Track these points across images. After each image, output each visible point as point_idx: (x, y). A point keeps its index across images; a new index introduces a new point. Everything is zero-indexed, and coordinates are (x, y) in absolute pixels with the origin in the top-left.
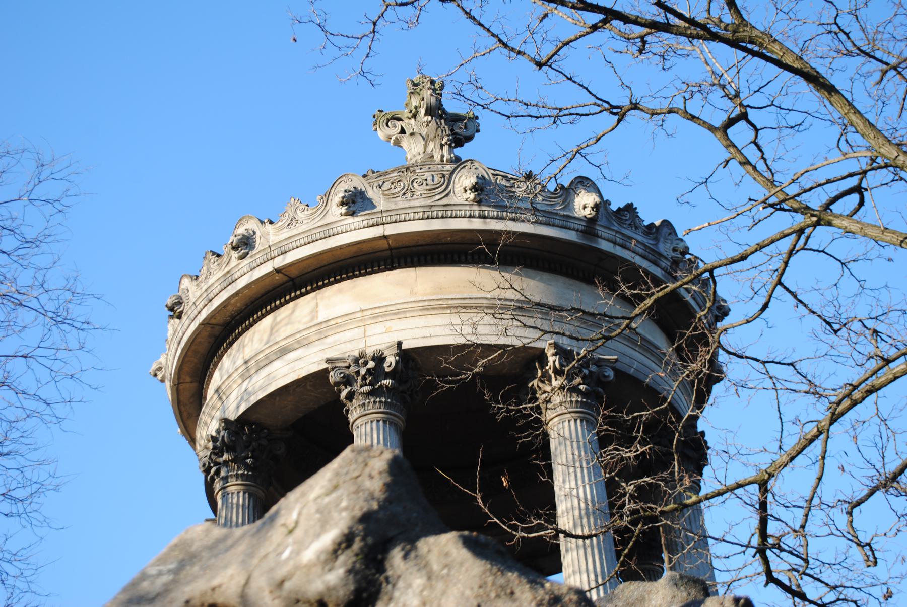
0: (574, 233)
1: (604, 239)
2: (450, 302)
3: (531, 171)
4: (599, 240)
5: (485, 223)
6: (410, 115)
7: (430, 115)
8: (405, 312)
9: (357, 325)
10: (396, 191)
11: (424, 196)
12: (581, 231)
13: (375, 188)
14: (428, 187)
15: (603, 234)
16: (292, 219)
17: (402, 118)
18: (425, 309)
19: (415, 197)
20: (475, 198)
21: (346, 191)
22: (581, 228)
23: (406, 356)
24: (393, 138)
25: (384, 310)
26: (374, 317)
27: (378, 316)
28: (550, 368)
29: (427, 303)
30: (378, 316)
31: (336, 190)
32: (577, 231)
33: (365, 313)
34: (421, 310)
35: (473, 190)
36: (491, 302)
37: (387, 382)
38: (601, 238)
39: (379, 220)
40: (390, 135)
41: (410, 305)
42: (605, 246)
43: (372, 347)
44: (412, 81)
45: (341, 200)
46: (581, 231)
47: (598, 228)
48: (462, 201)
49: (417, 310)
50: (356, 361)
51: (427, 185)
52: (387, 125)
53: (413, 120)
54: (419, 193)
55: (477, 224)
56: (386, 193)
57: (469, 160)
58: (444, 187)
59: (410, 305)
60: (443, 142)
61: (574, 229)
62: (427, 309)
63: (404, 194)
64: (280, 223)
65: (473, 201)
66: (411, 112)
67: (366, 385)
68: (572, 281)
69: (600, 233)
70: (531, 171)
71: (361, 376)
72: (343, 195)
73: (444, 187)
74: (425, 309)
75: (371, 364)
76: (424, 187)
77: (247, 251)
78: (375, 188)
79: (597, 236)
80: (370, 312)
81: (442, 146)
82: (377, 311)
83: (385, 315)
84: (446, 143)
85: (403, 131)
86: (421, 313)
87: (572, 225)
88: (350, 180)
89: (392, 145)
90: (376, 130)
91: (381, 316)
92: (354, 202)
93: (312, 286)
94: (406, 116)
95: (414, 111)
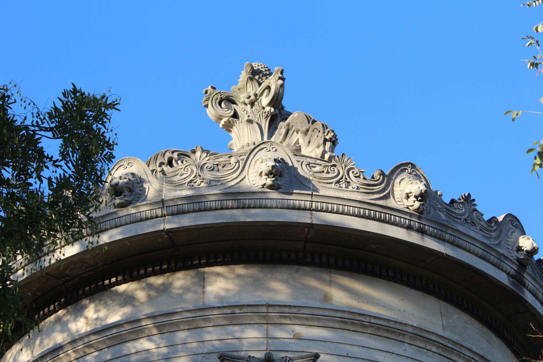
0: (505, 275)
1: (529, 291)
2: (373, 321)
3: (469, 194)
4: (526, 290)
5: (423, 239)
6: (247, 101)
7: (273, 107)
8: (319, 320)
9: (258, 321)
10: (331, 175)
11: (361, 190)
12: (512, 276)
13: (304, 166)
14: (365, 182)
15: (530, 284)
16: (196, 176)
17: (236, 101)
18: (343, 321)
19: (350, 188)
20: (419, 208)
21: (275, 160)
22: (512, 272)
24: (225, 119)
25: (295, 310)
26: (281, 316)
27: (286, 317)
29: (346, 315)
30: (286, 317)
31: (257, 157)
32: (508, 274)
33: (271, 310)
34: (338, 322)
35: (420, 198)
36: (416, 332)
38: (527, 288)
39: (308, 204)
40: (221, 116)
41: (327, 313)
42: (529, 297)
43: (280, 353)
44: (252, 67)
45: (270, 168)
46: (512, 276)
47: (525, 275)
49: (334, 321)
51: (364, 178)
52: (220, 104)
53: (249, 106)
54: (355, 186)
55: (414, 238)
56: (316, 175)
57: (407, 164)
58: (383, 185)
59: (327, 313)
60: (328, 137)
61: (505, 272)
62: (345, 323)
63: (338, 182)
64: (178, 176)
65: (417, 210)
66: (249, 97)
68: (485, 329)
69: (527, 283)
70: (469, 194)
72: (274, 164)
73: (383, 185)
74: (343, 321)
76: (361, 180)
77: (131, 199)
78: (304, 166)
79: (524, 285)
80: (277, 310)
81: (325, 140)
82: (287, 310)
83: (296, 318)
84: (331, 139)
85: (235, 116)
86: (337, 325)
87: (505, 267)
88: (274, 149)
89: (221, 126)
90: (207, 106)
91: (290, 318)
92: (281, 176)
93: (200, 260)
94: (242, 100)
95: (253, 97)
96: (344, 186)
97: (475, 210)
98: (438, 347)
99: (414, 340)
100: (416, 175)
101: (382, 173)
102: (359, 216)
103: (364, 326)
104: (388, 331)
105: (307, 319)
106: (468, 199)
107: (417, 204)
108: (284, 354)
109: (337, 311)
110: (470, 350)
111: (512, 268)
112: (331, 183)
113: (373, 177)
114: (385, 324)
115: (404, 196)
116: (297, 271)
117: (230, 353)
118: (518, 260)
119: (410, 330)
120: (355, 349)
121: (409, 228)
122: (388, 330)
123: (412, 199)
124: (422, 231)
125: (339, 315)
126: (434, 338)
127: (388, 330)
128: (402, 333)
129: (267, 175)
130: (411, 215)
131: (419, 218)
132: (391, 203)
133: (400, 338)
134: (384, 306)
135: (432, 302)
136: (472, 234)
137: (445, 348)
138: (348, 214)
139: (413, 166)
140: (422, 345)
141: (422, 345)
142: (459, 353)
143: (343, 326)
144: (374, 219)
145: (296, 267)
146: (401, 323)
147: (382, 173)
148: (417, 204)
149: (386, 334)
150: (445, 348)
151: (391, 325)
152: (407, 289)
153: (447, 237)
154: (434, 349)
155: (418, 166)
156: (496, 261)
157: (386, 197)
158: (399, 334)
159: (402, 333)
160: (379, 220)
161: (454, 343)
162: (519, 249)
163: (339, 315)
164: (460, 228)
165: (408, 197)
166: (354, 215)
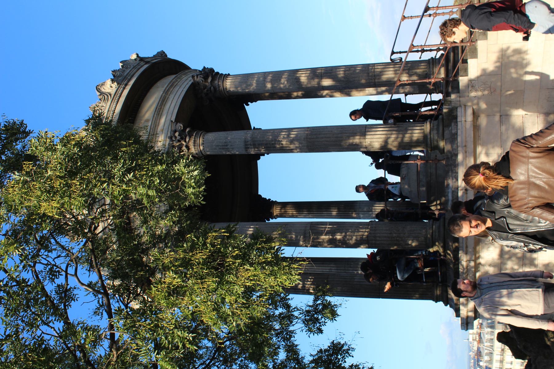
19: (105, 106)
22: (144, 63)
23: (177, 120)
25: (151, 130)
28: (202, 81)
29: (156, 113)
37: (188, 130)
41: (154, 120)
48: (115, 90)
57: (97, 88)
65: (118, 84)
71: (181, 140)
75: (177, 134)
83: (154, 130)
86: (159, 117)
96: (103, 108)
99: (168, 94)
100: (102, 85)
101: (100, 95)
102: (117, 103)
103: (161, 108)
104: (164, 101)
105: (155, 127)
106: (114, 71)
107: (116, 83)
109: (154, 116)
110: (173, 79)
111: (142, 63)
113: (100, 99)
115: (111, 88)
118: (140, 61)
119: (164, 94)
120: (177, 89)
121: (124, 88)
122: (163, 101)
123: (113, 85)
124: (126, 85)
125: (155, 116)
126: (168, 88)
127: (163, 101)
128: (165, 97)
130: (119, 87)
131: (121, 84)
132: (113, 93)
133: (167, 98)
134: (153, 103)
135: (152, 90)
136: (128, 71)
137: (172, 86)
138: (116, 107)
139: (98, 86)
140: (170, 92)
141: (170, 92)
142: (174, 83)
143: (160, 115)
144: (119, 99)
146: (161, 97)
147: (100, 95)
148: (116, 83)
149: (165, 102)
150: (172, 86)
152: (148, 94)
153: (129, 78)
154: (172, 89)
155: (98, 84)
156: (140, 66)
157: (110, 95)
159: (165, 97)
160: (120, 97)
161: (170, 83)
162: (135, 60)
163: (155, 116)
164: (126, 74)
165: (112, 87)
166: (116, 105)
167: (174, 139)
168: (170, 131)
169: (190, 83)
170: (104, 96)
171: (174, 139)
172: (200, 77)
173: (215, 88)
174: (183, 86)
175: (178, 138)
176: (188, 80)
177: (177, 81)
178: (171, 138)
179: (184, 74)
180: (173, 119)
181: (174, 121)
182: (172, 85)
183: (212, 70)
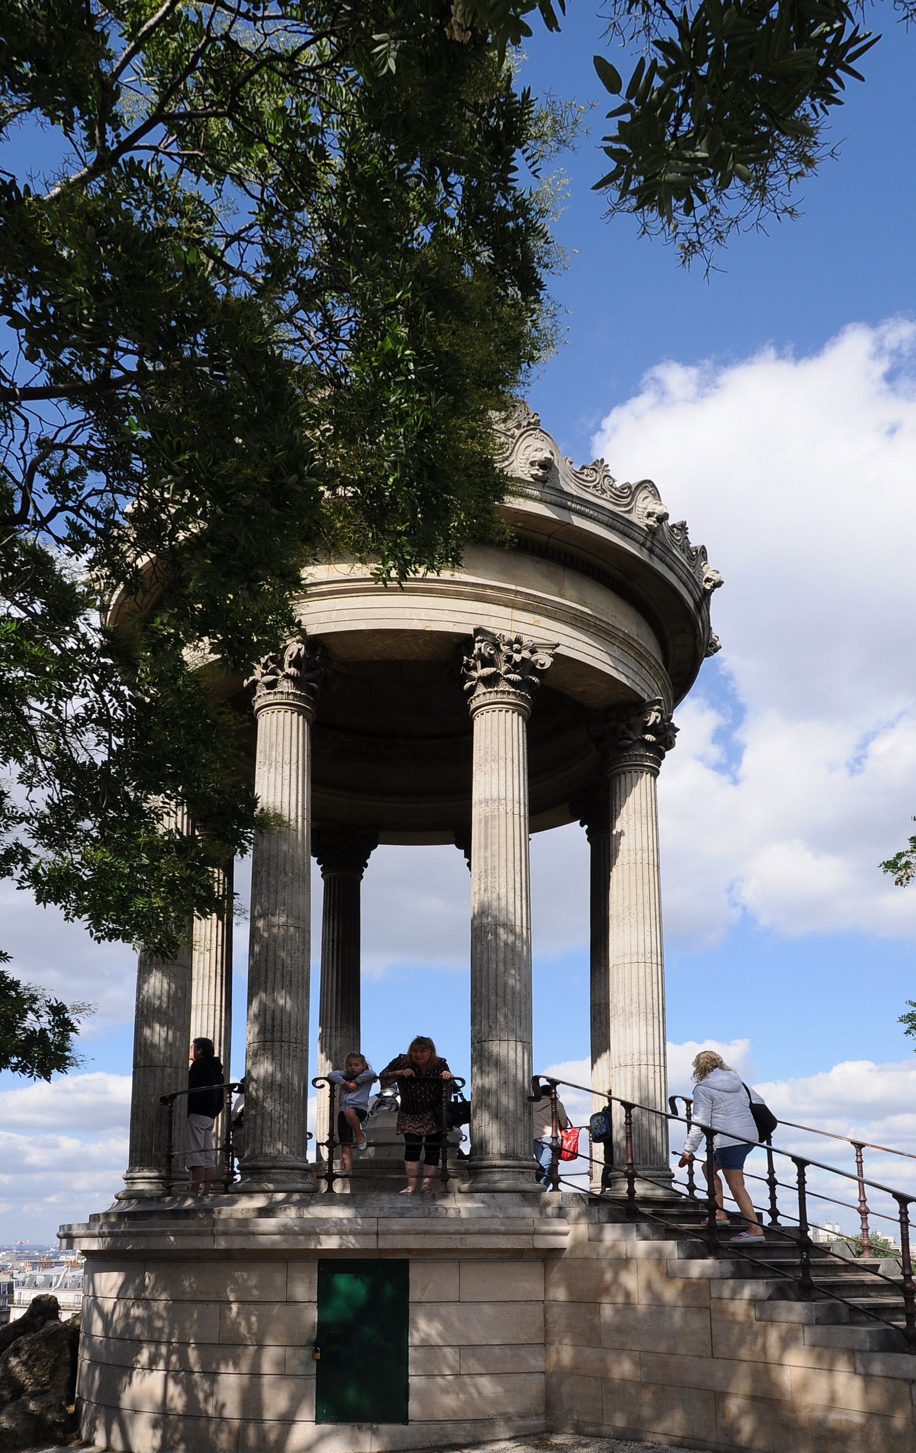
23: (558, 658)
29: (578, 614)
50: (510, 644)
63: (595, 487)
67: (514, 673)
73: (629, 499)
75: (526, 654)
97: (687, 538)
98: (636, 653)
103: (590, 626)
104: (606, 633)
108: (530, 638)
112: (589, 487)
114: (606, 626)
116: (538, 562)
117: (487, 629)
118: (704, 589)
122: (607, 632)
127: (607, 632)
129: (539, 465)
132: (633, 517)
137: (640, 655)
139: (653, 485)
142: (648, 661)
145: (537, 559)
150: (640, 655)
151: (609, 628)
157: (629, 512)
158: (613, 637)
161: (648, 652)
167: (516, 646)
168: (536, 640)
169: (645, 697)
170: (627, 497)
171: (516, 646)
172: (657, 718)
173: (628, 748)
174: (637, 680)
175: (517, 657)
176: (650, 692)
177: (651, 667)
178: (518, 641)
179: (664, 686)
180: (559, 650)
181: (557, 650)
182: (641, 656)
183: (670, 745)
